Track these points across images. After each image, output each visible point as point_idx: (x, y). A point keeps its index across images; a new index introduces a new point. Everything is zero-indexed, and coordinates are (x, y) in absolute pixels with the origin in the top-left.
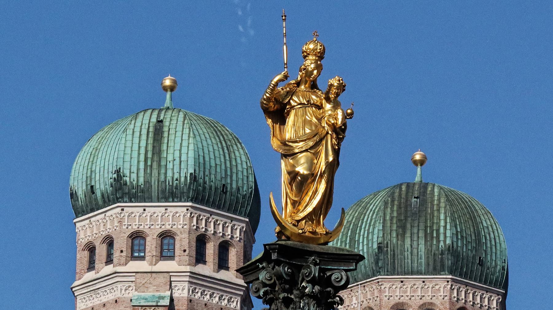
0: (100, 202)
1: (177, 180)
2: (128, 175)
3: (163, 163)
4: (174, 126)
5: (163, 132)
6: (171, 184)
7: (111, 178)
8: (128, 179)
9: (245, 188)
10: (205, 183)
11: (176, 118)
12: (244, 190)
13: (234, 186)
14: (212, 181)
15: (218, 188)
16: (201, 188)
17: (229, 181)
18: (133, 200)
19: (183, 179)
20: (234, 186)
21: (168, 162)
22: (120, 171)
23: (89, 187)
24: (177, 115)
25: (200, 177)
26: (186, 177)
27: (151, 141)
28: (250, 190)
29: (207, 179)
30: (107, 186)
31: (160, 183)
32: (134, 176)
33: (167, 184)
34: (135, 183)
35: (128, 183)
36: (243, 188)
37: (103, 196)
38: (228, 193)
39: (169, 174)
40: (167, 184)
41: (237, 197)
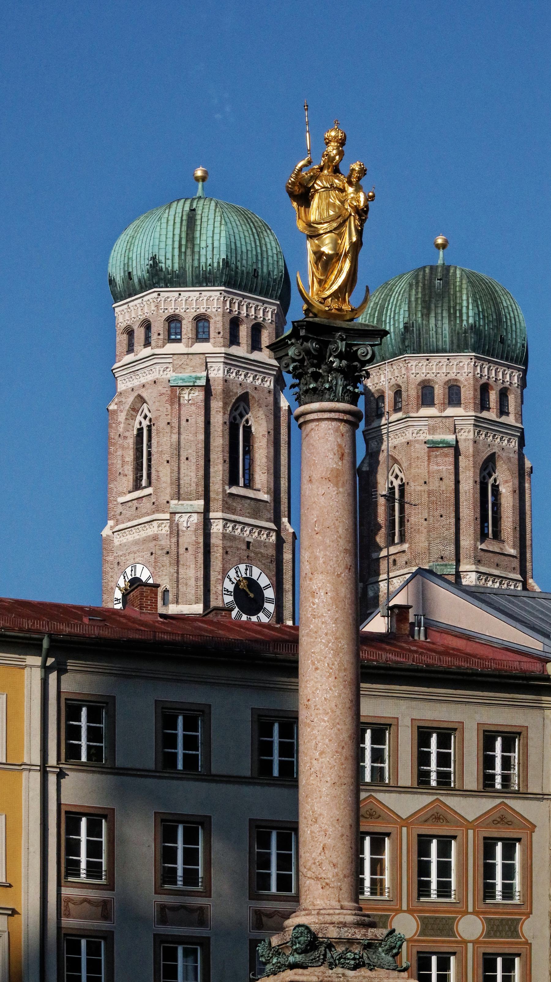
1: (210, 265)
2: (163, 261)
3: (196, 249)
4: (206, 215)
5: (195, 220)
6: (204, 269)
7: (147, 265)
8: (163, 265)
10: (237, 267)
11: (207, 206)
18: (168, 285)
19: (215, 265)
21: (201, 249)
22: (155, 258)
23: (127, 274)
24: (208, 203)
26: (218, 263)
27: (184, 228)
30: (144, 273)
31: (194, 268)
32: (169, 262)
33: (201, 269)
34: (170, 269)
35: (164, 269)
37: (140, 281)
39: (203, 260)
40: (201, 269)
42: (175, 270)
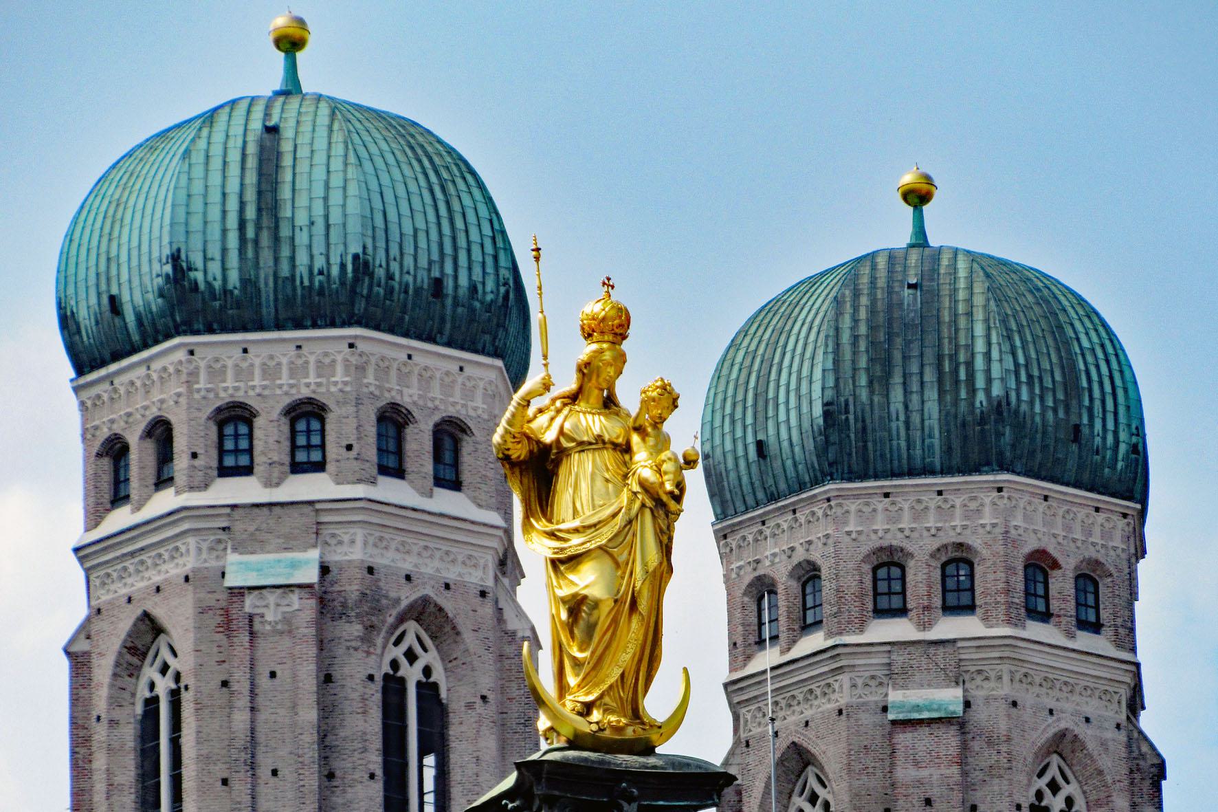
1: (321, 273)
2: (199, 264)
3: (285, 232)
5: (279, 155)
6: (306, 283)
8: (199, 276)
9: (490, 285)
10: (390, 277)
12: (488, 289)
13: (463, 281)
14: (408, 273)
15: (422, 288)
16: (381, 291)
17: (449, 269)
19: (335, 271)
20: (463, 281)
21: (297, 230)
22: (179, 257)
23: (105, 300)
24: (312, 109)
25: (377, 263)
26: (343, 266)
27: (251, 178)
28: (502, 290)
29: (395, 267)
30: (150, 296)
31: (280, 282)
32: (215, 268)
33: (298, 283)
34: (217, 284)
35: (202, 286)
36: (484, 284)
38: (449, 302)
39: (302, 259)
40: (298, 283)
41: (472, 310)
42: (230, 287)
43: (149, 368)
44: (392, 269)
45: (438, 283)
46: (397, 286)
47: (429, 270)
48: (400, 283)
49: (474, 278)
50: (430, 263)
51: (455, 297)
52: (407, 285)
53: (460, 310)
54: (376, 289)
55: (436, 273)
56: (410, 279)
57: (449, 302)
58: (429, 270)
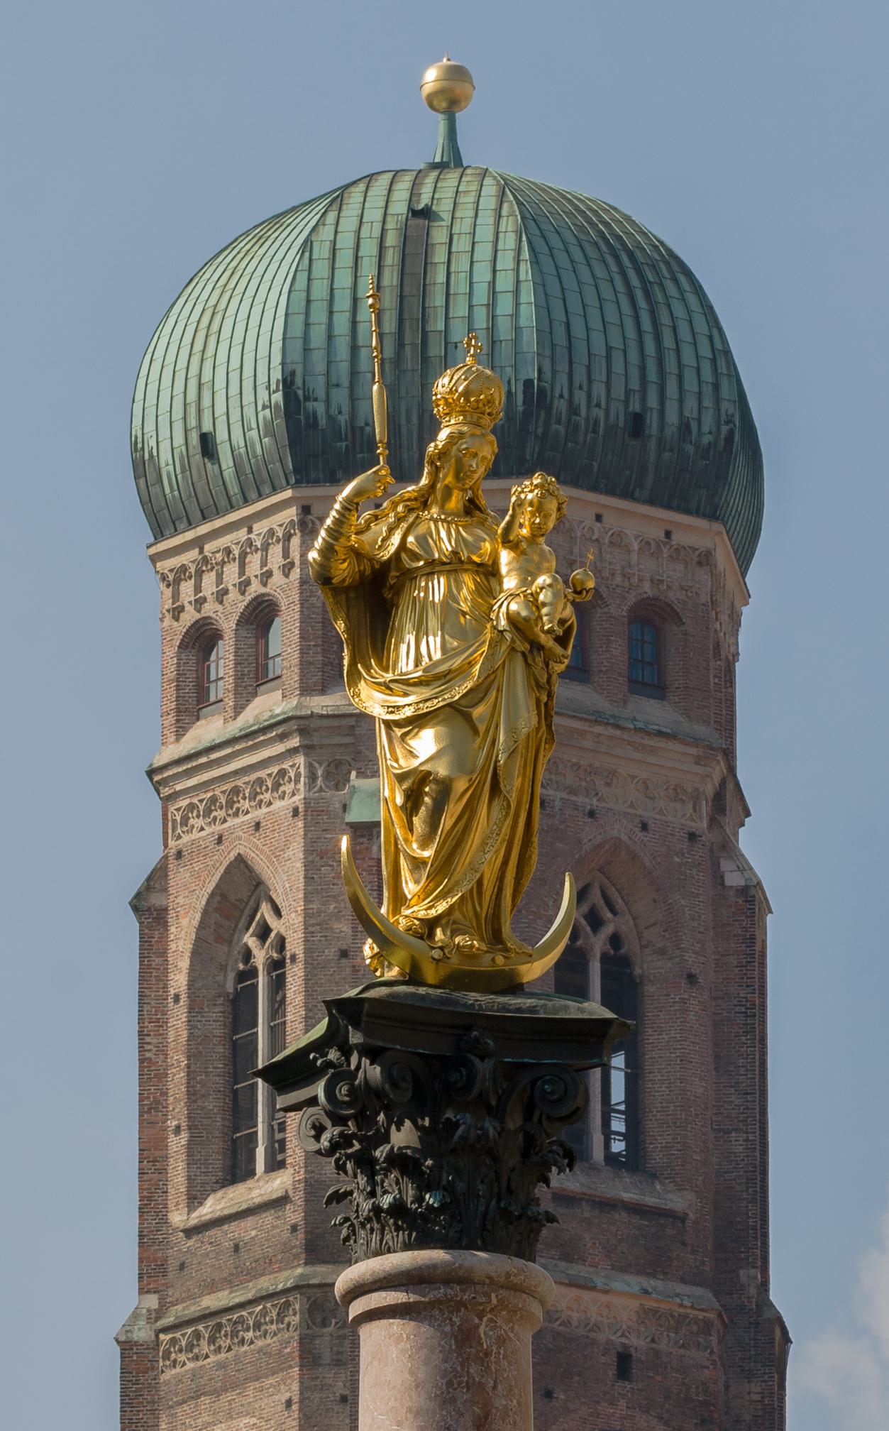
0: (234, 489)
2: (320, 393)
7: (264, 407)
8: (320, 408)
9: (708, 423)
10: (573, 410)
12: (706, 429)
13: (672, 417)
14: (598, 405)
16: (562, 429)
17: (653, 402)
20: (672, 417)
22: (292, 382)
23: (195, 439)
25: (557, 394)
29: (580, 397)
34: (343, 419)
35: (323, 422)
36: (699, 420)
38: (653, 444)
43: (250, 531)
44: (577, 401)
45: (637, 423)
46: (583, 423)
47: (626, 402)
48: (587, 419)
49: (687, 414)
50: (628, 392)
51: (660, 440)
52: (596, 422)
53: (666, 455)
54: (555, 427)
55: (635, 406)
56: (601, 414)
57: (653, 444)
58: (626, 402)
